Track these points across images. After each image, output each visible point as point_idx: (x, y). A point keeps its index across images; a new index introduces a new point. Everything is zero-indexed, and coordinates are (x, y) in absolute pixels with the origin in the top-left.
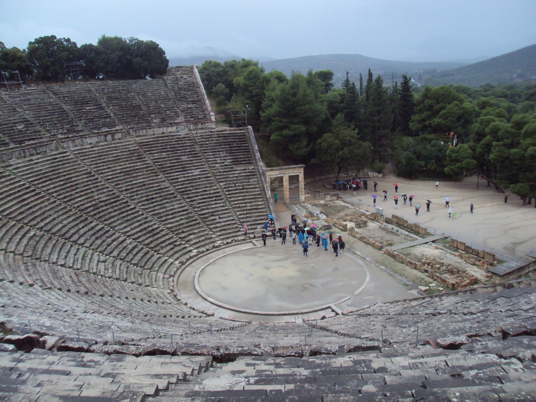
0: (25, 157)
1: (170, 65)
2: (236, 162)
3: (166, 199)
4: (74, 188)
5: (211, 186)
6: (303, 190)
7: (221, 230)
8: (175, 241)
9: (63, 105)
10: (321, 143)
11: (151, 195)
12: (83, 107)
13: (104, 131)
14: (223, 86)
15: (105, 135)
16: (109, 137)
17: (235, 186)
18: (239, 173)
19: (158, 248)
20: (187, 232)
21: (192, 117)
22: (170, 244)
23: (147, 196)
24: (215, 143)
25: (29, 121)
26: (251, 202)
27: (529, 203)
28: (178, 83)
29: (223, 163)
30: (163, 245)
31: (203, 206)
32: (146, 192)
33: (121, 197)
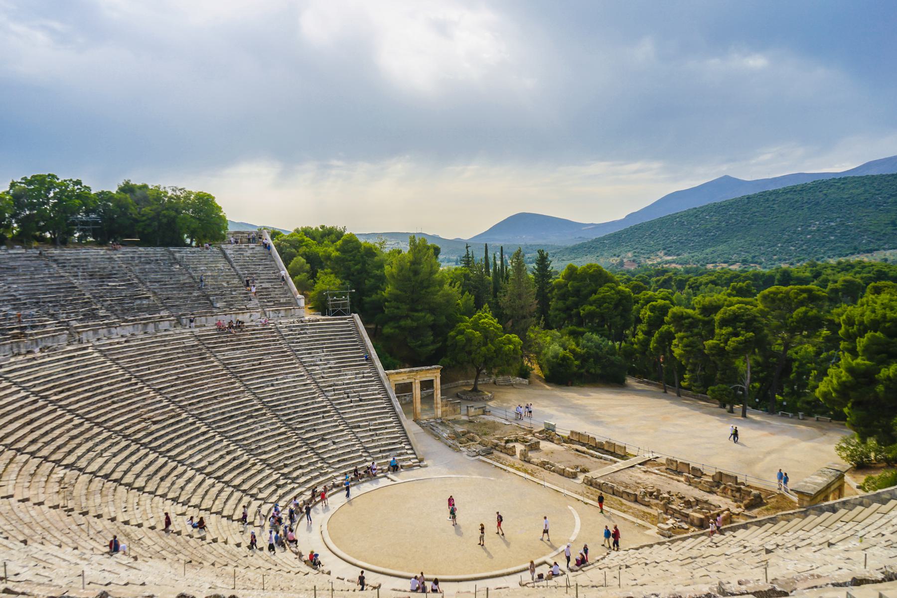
0: (19, 354)
1: (231, 229)
2: (343, 364)
3: (252, 417)
4: (109, 402)
5: (313, 398)
6: (439, 401)
7: (339, 462)
8: (277, 480)
9: (71, 278)
10: (454, 337)
11: (229, 412)
12: (103, 282)
13: (142, 317)
14: (303, 260)
15: (144, 324)
16: (151, 328)
17: (348, 397)
18: (350, 379)
19: (254, 491)
20: (290, 464)
21: (271, 301)
22: (270, 484)
23: (223, 413)
24: (310, 337)
25: (19, 299)
26: (375, 419)
27: (731, 411)
28: (242, 254)
29: (326, 364)
30: (261, 486)
31: (307, 426)
32: (220, 408)
33: (184, 416)
